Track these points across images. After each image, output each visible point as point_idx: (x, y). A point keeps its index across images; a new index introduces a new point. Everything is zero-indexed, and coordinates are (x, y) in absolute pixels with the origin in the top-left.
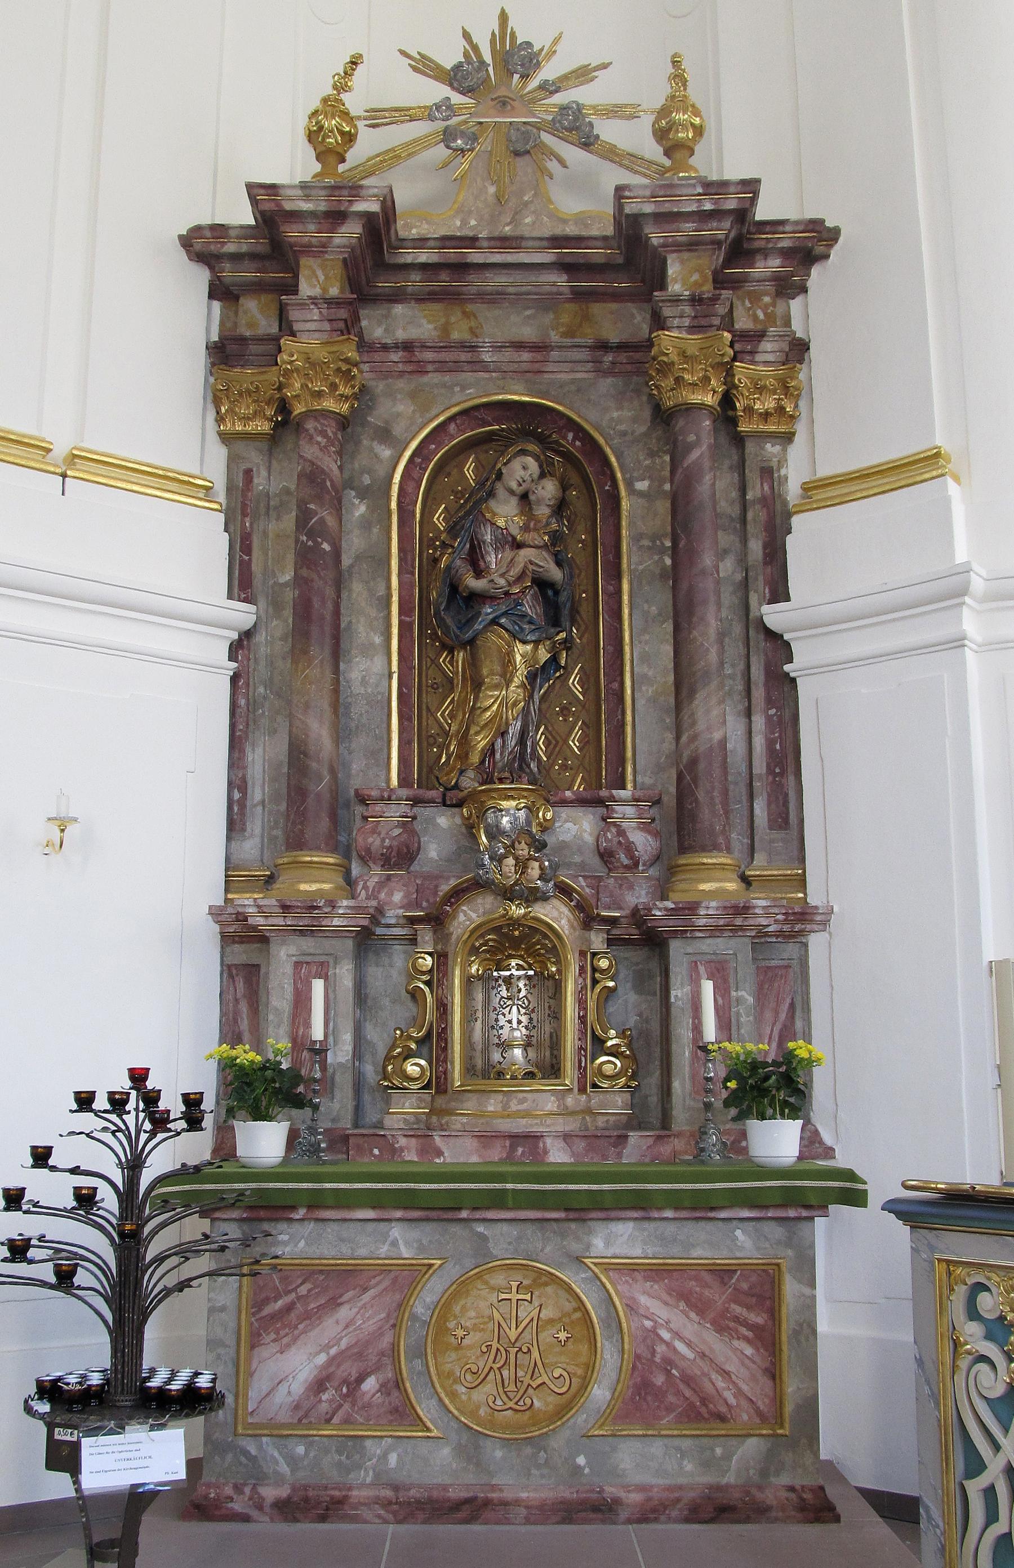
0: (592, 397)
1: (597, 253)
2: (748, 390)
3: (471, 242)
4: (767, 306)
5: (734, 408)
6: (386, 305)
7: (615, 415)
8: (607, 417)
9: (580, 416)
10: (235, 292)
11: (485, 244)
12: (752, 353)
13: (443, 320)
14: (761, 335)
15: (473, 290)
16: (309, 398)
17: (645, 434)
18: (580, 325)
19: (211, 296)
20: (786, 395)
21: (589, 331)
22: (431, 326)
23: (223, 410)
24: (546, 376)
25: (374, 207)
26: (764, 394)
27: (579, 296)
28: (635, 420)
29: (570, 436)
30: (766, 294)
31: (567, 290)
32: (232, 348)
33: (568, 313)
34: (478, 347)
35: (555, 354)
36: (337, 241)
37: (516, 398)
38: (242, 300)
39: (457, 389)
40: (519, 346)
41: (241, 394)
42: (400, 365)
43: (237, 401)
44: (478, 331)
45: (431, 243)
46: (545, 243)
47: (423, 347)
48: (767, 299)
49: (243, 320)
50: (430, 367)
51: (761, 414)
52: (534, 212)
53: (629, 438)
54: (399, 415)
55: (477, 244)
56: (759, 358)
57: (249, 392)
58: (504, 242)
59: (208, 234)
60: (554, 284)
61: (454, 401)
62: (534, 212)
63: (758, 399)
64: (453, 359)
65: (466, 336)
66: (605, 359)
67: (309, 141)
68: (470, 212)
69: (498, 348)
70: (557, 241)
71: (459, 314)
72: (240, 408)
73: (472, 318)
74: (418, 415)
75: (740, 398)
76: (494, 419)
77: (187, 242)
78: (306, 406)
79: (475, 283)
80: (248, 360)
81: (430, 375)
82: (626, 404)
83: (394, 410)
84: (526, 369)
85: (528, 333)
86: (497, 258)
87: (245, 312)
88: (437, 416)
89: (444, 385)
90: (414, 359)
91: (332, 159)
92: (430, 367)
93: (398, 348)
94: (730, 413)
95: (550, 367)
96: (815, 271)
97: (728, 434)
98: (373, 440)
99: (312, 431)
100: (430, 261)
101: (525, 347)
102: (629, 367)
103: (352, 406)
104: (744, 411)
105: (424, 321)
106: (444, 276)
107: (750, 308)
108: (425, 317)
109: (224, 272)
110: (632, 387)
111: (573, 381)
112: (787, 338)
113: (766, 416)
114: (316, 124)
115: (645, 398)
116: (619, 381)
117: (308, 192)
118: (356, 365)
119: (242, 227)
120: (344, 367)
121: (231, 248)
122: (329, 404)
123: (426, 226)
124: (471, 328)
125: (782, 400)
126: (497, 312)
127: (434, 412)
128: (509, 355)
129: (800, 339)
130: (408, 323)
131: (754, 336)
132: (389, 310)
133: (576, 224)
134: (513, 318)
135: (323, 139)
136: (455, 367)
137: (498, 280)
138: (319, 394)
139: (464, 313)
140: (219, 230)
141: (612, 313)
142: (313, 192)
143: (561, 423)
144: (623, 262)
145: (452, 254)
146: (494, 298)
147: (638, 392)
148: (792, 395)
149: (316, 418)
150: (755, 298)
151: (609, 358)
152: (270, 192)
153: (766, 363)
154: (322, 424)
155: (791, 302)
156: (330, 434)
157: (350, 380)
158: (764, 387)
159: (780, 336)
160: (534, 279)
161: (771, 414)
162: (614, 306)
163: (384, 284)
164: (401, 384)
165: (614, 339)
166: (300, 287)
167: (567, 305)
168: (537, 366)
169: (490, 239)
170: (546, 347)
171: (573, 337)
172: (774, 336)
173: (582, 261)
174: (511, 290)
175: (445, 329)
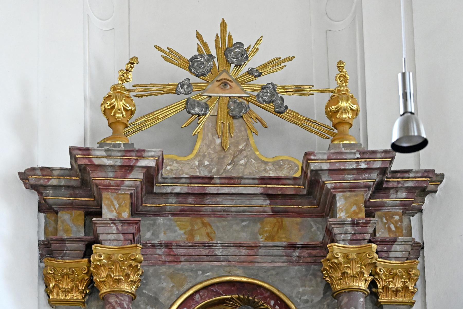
0: (286, 278)
1: (289, 188)
2: (385, 276)
3: (210, 180)
4: (397, 222)
5: (376, 287)
6: (153, 218)
7: (301, 290)
8: (295, 291)
9: (279, 291)
10: (55, 209)
11: (218, 181)
12: (388, 252)
13: (190, 228)
14: (394, 241)
15: (209, 208)
16: (111, 283)
17: (320, 302)
18: (278, 232)
19: (40, 210)
20: (409, 279)
21: (284, 236)
22: (182, 232)
23: (51, 286)
24: (256, 264)
25: (152, 164)
26: (395, 278)
27: (276, 213)
28: (313, 293)
29: (272, 302)
30: (397, 214)
31: (269, 210)
32: (55, 245)
33: (270, 224)
34: (213, 246)
35: (262, 251)
36: (127, 183)
37: (238, 279)
38: (59, 214)
39: (200, 272)
40: (239, 246)
41: (63, 276)
42: (163, 257)
43: (61, 280)
44: (212, 235)
45: (183, 181)
46: (256, 182)
47: (177, 246)
48: (397, 218)
49: (60, 228)
50: (182, 258)
51: (393, 291)
52: (245, 157)
53: (309, 304)
54: (163, 289)
55: (213, 181)
56: (392, 255)
57: (68, 275)
58: (231, 180)
59: (39, 172)
60: (261, 206)
61: (199, 279)
62: (245, 157)
63: (392, 282)
64: (197, 253)
65: (206, 240)
66: (294, 254)
67: (104, 114)
68: (204, 156)
69: (225, 246)
70: (264, 180)
71: (200, 225)
72: (63, 285)
73: (209, 227)
74: (175, 289)
75: (381, 281)
76: (223, 292)
77: (24, 176)
78: (110, 288)
79: (209, 204)
80: (66, 253)
81: (182, 263)
82: (307, 283)
83: (160, 285)
84: (244, 260)
85: (244, 237)
86: (226, 190)
87: (63, 222)
88: (188, 290)
89: (192, 271)
90: (172, 253)
91: (121, 127)
92: (182, 258)
93: (162, 246)
94: (374, 290)
95: (259, 259)
96: (427, 199)
97: (372, 302)
98: (147, 305)
99: (114, 304)
100: (182, 192)
101: (243, 247)
102: (309, 260)
103: (137, 287)
104: (383, 289)
105: (177, 228)
106: (190, 200)
107: (386, 223)
108: (178, 226)
109: (48, 196)
110: (311, 272)
111: (274, 268)
112: (409, 243)
113: (396, 292)
114: (110, 105)
115: (319, 279)
116: (303, 268)
117: (109, 153)
118: (140, 262)
119: (61, 169)
120: (134, 264)
121: (54, 182)
122: (126, 287)
123: (176, 165)
124: (207, 233)
125: (407, 282)
126: (225, 223)
127: (186, 287)
128: (233, 250)
129: (418, 243)
130: (167, 229)
131: (389, 242)
132: (155, 221)
133: (273, 165)
134: (235, 227)
135: (114, 115)
136: (199, 259)
137: (227, 202)
138: (119, 281)
139: (203, 223)
140: (47, 171)
141: (297, 224)
142: (113, 153)
143: (267, 294)
144: (306, 195)
145: (196, 188)
146: (222, 214)
147: (315, 275)
148: (413, 279)
149: (116, 296)
150: (390, 217)
151: (297, 253)
152: (85, 152)
153: (396, 258)
154: (121, 300)
155: (411, 218)
156: (125, 306)
157: (136, 272)
158: (396, 274)
159: (405, 242)
160: (248, 203)
161: (400, 291)
162: (299, 220)
163: (152, 205)
164: (163, 269)
165: (300, 243)
166: (104, 211)
167: (269, 219)
168: (251, 258)
169: (220, 178)
170: (257, 247)
171: (273, 240)
172: (402, 242)
173: (279, 193)
174: (233, 209)
175: (191, 234)
